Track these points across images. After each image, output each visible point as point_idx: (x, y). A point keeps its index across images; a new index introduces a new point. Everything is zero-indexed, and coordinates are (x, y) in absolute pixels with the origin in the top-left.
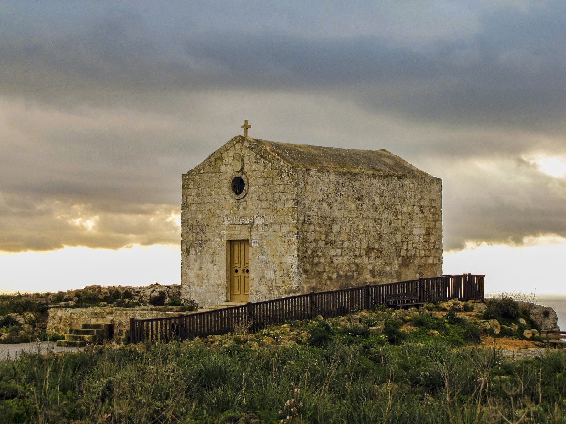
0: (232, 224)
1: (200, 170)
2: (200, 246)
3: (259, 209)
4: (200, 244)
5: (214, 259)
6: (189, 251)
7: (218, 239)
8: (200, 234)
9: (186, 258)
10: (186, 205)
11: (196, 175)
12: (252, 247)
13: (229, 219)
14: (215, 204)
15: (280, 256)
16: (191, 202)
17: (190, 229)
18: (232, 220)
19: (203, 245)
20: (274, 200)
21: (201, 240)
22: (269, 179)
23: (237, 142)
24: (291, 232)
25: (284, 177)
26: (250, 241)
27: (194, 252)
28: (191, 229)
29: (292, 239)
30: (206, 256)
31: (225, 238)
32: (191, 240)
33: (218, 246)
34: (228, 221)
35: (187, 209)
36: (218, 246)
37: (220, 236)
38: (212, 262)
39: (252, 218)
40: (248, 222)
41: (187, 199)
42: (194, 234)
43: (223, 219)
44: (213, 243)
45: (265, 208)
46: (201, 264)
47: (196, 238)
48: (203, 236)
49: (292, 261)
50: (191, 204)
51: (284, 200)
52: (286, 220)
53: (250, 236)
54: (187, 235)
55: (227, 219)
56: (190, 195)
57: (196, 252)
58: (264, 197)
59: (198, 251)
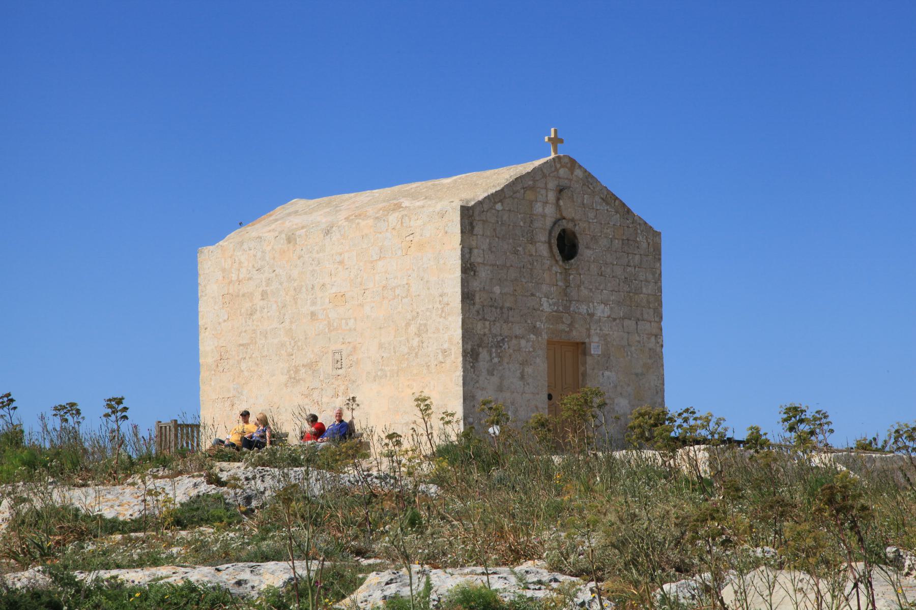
0: (556, 312)
1: (495, 203)
2: (498, 345)
3: (602, 290)
4: (498, 342)
5: (526, 370)
6: (478, 355)
7: (532, 336)
8: (498, 324)
9: (471, 367)
10: (470, 264)
11: (487, 211)
12: (591, 355)
13: (551, 301)
14: (525, 270)
15: (637, 375)
16: (480, 260)
17: (478, 312)
18: (554, 304)
19: (504, 344)
20: (625, 278)
21: (501, 335)
22: (617, 241)
23: (562, 166)
24: (653, 335)
25: (641, 241)
26: (587, 345)
27: (487, 358)
28: (481, 312)
29: (654, 348)
30: (510, 366)
31: (545, 336)
32: (482, 333)
33: (531, 350)
34: (550, 305)
35: (472, 273)
36: (531, 350)
37: (534, 330)
38: (522, 377)
39: (591, 304)
40: (585, 311)
41: (470, 253)
42: (487, 323)
43: (541, 301)
44: (523, 342)
45: (612, 289)
46: (502, 378)
47: (490, 330)
48: (503, 327)
49: (656, 386)
50: (479, 263)
51: (642, 281)
52: (646, 316)
53: (589, 336)
54: (472, 323)
55: (548, 302)
56: (477, 248)
57: (491, 356)
58: (608, 270)
59: (494, 355)
